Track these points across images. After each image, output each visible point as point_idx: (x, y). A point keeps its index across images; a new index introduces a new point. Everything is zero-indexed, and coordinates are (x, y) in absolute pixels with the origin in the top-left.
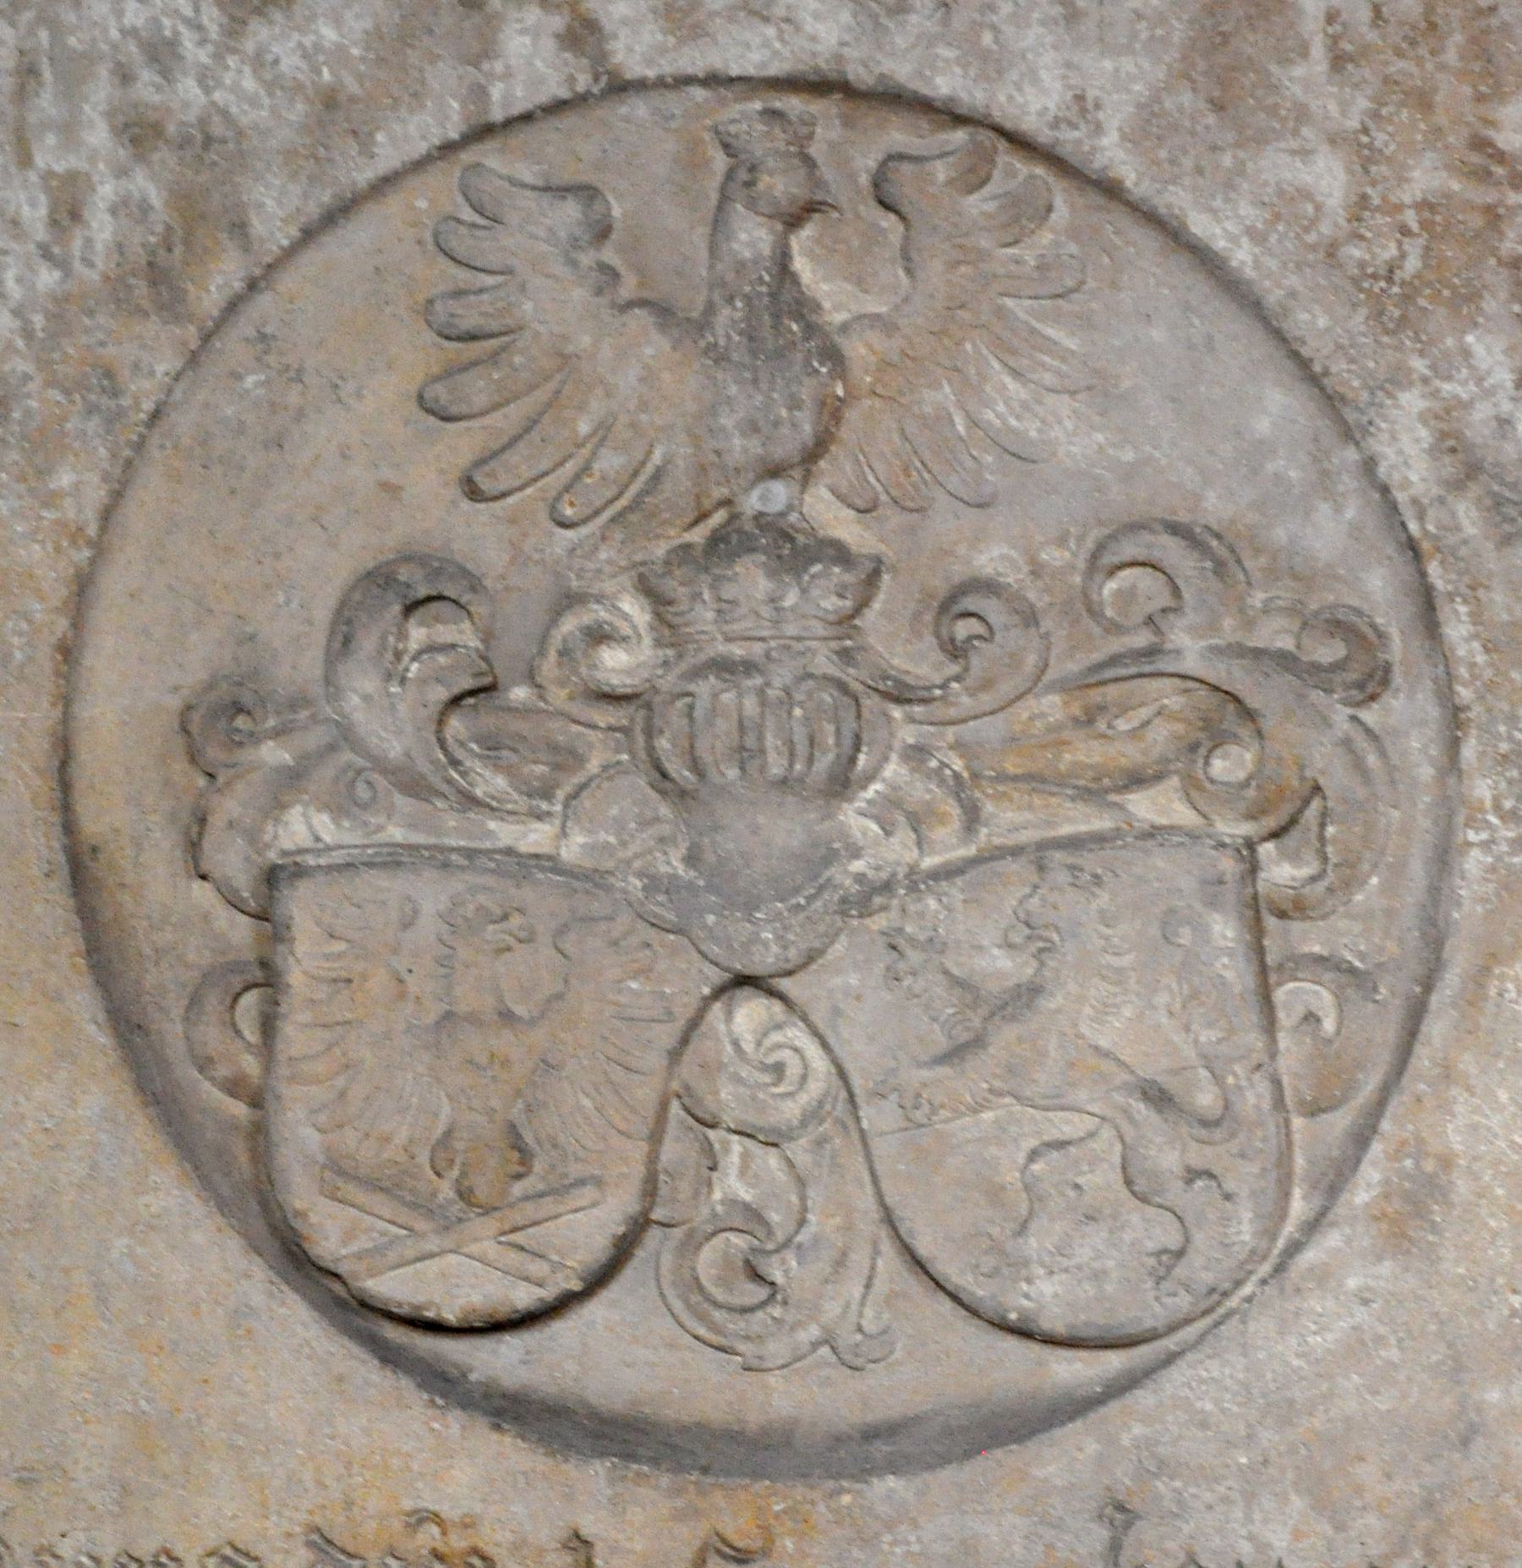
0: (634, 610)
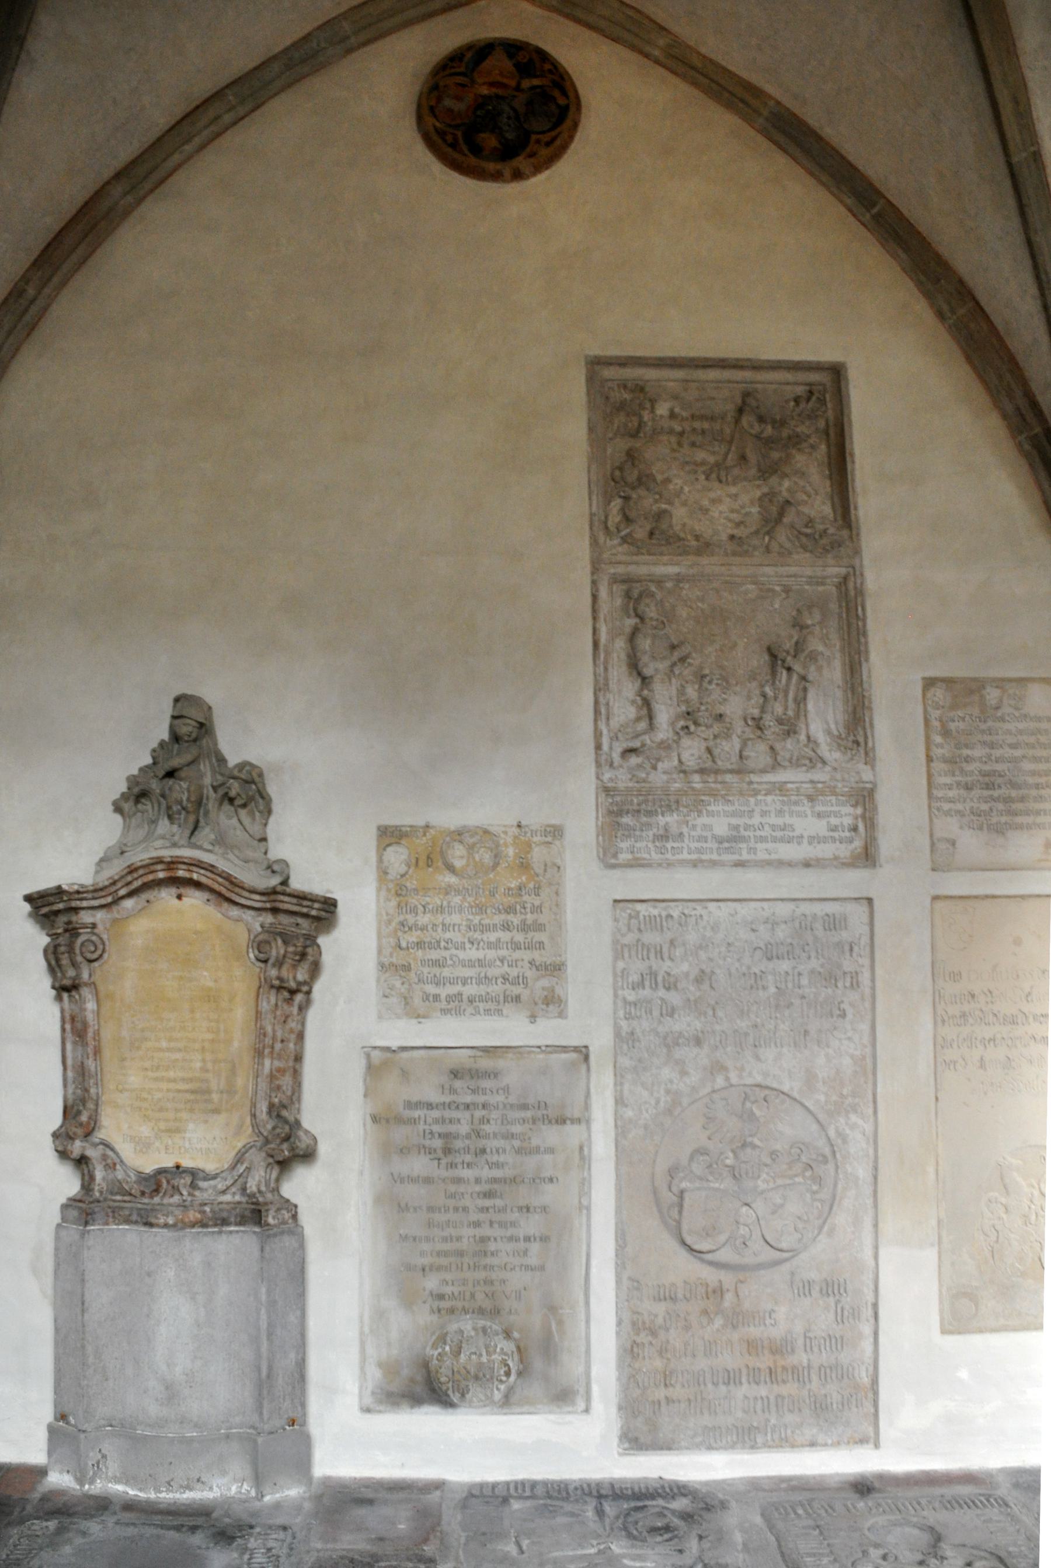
0: (731, 1155)
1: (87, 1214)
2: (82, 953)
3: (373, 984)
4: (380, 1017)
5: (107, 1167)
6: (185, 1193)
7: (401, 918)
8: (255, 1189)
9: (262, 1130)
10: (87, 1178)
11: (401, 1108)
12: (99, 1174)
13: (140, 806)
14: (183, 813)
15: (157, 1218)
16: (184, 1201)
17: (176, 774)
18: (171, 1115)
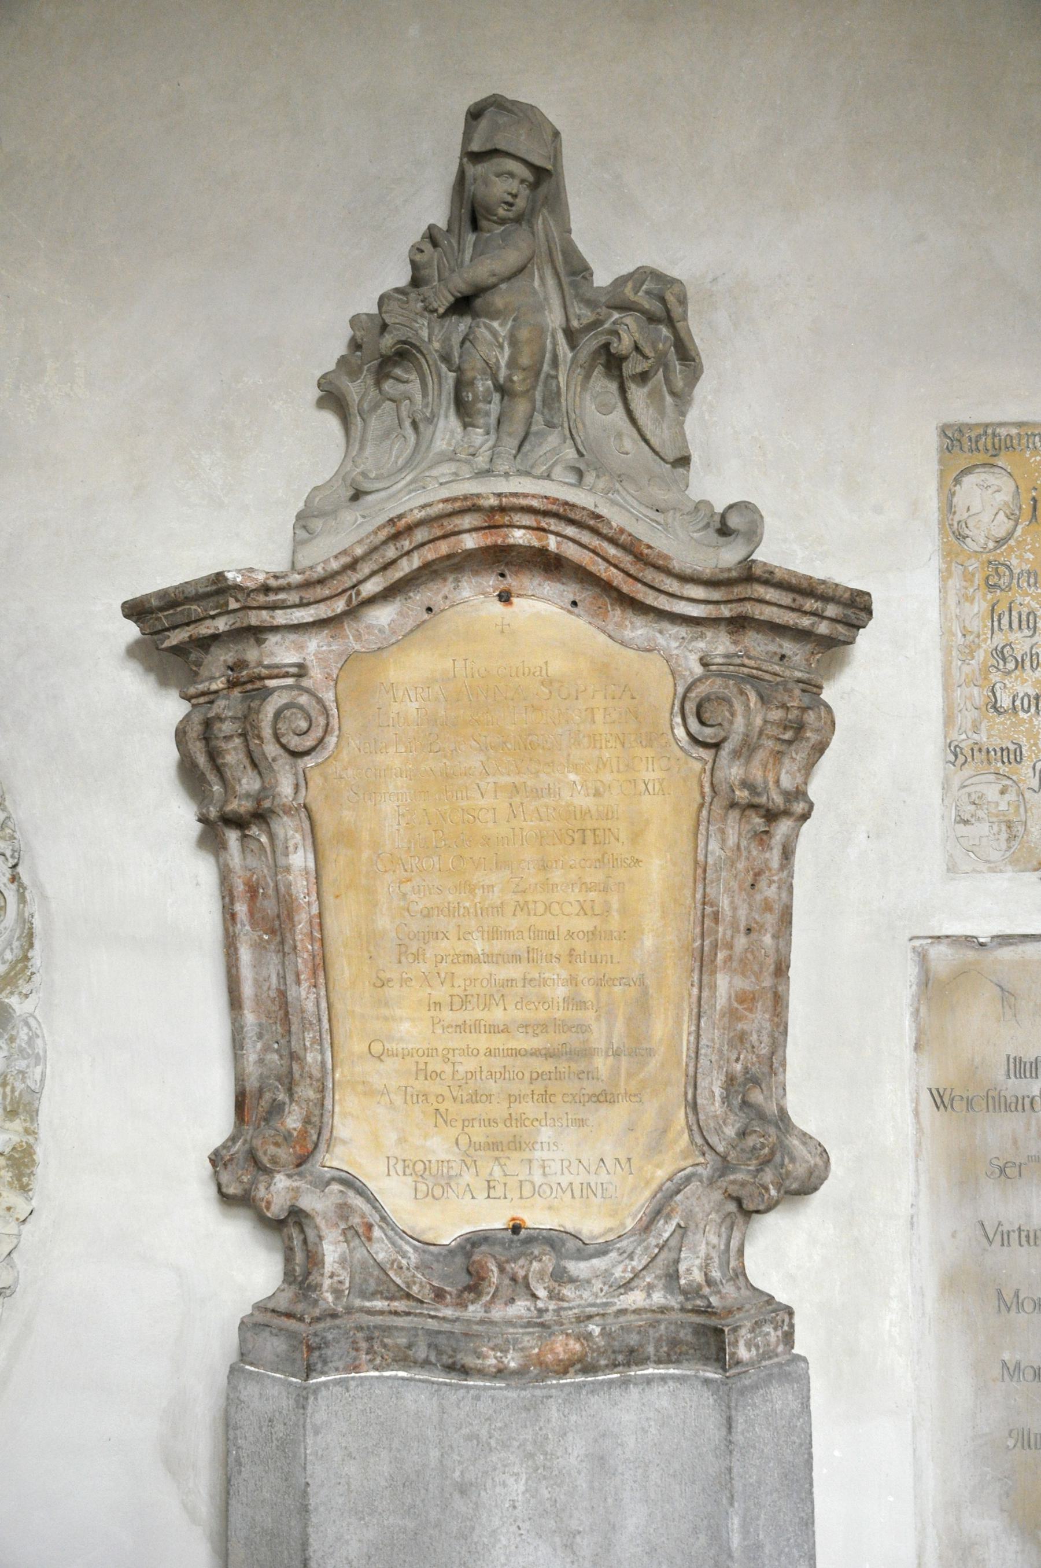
1: (310, 1349)
2: (277, 737)
3: (937, 794)
4: (952, 869)
5: (350, 1233)
6: (542, 1293)
7: (999, 640)
8: (698, 1276)
9: (713, 1140)
10: (299, 1257)
11: (1001, 1075)
12: (332, 1251)
13: (388, 386)
14: (496, 397)
15: (479, 1355)
16: (541, 1312)
17: (478, 302)
18: (498, 1109)
